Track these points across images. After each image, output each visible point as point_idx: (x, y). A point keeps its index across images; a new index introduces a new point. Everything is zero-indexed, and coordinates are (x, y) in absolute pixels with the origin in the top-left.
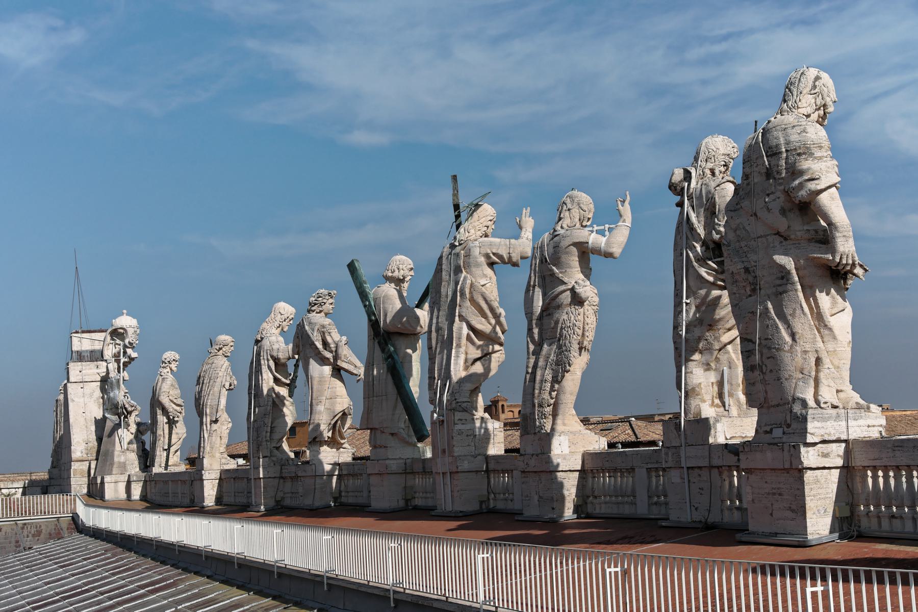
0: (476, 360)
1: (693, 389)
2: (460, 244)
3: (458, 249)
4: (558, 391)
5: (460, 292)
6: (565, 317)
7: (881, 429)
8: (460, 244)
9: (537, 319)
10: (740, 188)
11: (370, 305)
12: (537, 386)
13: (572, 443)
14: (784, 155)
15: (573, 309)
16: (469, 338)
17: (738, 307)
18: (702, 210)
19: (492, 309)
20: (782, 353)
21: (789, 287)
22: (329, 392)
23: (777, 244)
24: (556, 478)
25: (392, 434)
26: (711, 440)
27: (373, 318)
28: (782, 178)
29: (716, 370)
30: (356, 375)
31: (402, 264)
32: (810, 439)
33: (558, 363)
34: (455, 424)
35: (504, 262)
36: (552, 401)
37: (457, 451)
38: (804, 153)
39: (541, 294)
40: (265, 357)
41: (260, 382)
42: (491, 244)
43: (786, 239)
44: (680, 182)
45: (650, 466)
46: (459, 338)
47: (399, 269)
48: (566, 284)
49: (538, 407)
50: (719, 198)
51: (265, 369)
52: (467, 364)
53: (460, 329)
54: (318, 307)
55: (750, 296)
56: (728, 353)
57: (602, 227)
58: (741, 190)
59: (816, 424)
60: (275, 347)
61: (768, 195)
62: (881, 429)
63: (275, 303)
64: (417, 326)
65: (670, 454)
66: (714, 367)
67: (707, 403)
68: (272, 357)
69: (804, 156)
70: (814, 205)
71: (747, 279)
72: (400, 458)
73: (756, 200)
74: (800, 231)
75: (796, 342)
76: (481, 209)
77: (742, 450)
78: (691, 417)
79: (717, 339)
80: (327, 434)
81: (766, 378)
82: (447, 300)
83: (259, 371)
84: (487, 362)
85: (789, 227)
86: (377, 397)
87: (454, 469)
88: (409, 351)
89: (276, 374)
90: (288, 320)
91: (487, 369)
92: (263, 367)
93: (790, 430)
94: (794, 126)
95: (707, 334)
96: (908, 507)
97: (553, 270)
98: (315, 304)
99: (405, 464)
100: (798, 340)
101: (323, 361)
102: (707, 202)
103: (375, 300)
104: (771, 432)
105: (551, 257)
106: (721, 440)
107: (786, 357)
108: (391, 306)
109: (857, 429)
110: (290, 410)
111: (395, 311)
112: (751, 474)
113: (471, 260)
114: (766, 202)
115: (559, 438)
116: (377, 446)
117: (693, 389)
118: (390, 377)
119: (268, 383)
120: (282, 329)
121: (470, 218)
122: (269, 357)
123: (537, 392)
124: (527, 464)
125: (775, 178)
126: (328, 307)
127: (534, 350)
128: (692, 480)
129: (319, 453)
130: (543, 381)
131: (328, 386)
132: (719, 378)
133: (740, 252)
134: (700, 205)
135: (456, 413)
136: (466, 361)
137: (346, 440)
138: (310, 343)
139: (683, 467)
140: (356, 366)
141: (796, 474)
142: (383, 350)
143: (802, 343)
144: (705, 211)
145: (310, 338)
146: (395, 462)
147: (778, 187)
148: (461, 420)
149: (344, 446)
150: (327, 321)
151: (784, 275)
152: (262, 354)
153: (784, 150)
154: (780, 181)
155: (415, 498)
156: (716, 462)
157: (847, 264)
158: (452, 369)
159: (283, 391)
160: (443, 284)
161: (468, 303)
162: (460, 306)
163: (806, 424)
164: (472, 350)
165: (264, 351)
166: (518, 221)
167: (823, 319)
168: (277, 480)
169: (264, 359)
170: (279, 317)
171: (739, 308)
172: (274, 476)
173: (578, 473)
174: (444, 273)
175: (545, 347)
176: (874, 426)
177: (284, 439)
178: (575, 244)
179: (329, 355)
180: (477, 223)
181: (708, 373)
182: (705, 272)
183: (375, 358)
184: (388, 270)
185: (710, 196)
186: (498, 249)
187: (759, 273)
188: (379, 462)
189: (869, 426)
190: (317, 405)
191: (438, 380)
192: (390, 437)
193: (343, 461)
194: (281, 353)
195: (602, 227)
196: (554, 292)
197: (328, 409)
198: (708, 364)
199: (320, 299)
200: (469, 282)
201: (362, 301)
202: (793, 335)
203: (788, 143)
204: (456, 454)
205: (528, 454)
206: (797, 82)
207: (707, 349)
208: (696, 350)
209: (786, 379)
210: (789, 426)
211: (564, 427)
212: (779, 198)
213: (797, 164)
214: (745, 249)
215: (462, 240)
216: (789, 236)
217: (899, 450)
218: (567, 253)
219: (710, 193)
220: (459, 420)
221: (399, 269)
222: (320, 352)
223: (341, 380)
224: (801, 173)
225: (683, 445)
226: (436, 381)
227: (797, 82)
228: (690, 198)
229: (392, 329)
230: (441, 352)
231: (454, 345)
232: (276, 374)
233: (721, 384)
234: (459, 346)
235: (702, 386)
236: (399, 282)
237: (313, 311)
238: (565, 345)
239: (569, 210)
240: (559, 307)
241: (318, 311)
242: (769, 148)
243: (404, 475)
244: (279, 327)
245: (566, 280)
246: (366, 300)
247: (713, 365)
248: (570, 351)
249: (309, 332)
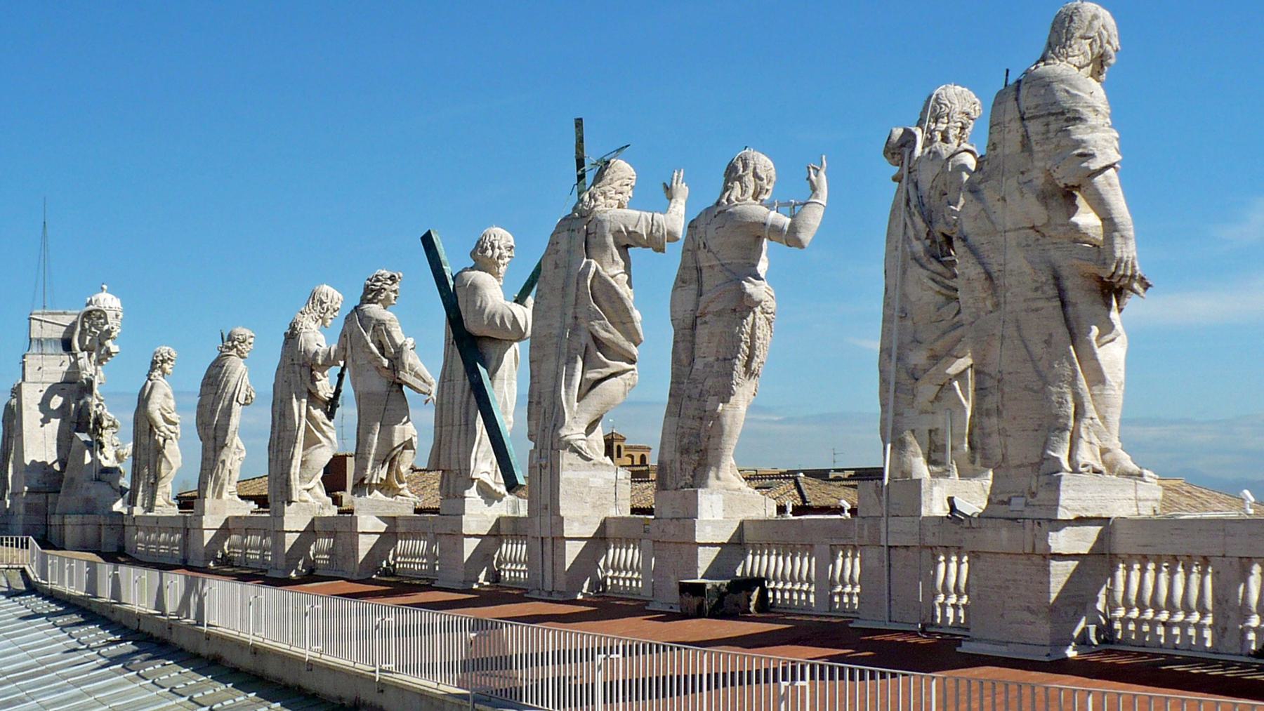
7: (1155, 504)
10: (984, 161)
13: (728, 506)
26: (925, 512)
30: (424, 393)
32: (1062, 514)
58: (986, 163)
59: (1072, 494)
62: (1155, 504)
65: (866, 527)
93: (1034, 501)
104: (1008, 503)
124: (663, 531)
137: (406, 485)
139: (883, 546)
141: (1036, 559)
149: (401, 492)
156: (930, 540)
157: (1124, 276)
176: (1147, 500)
186: (636, 227)
199: (379, 284)
200: (592, 270)
210: (1033, 495)
225: (885, 515)
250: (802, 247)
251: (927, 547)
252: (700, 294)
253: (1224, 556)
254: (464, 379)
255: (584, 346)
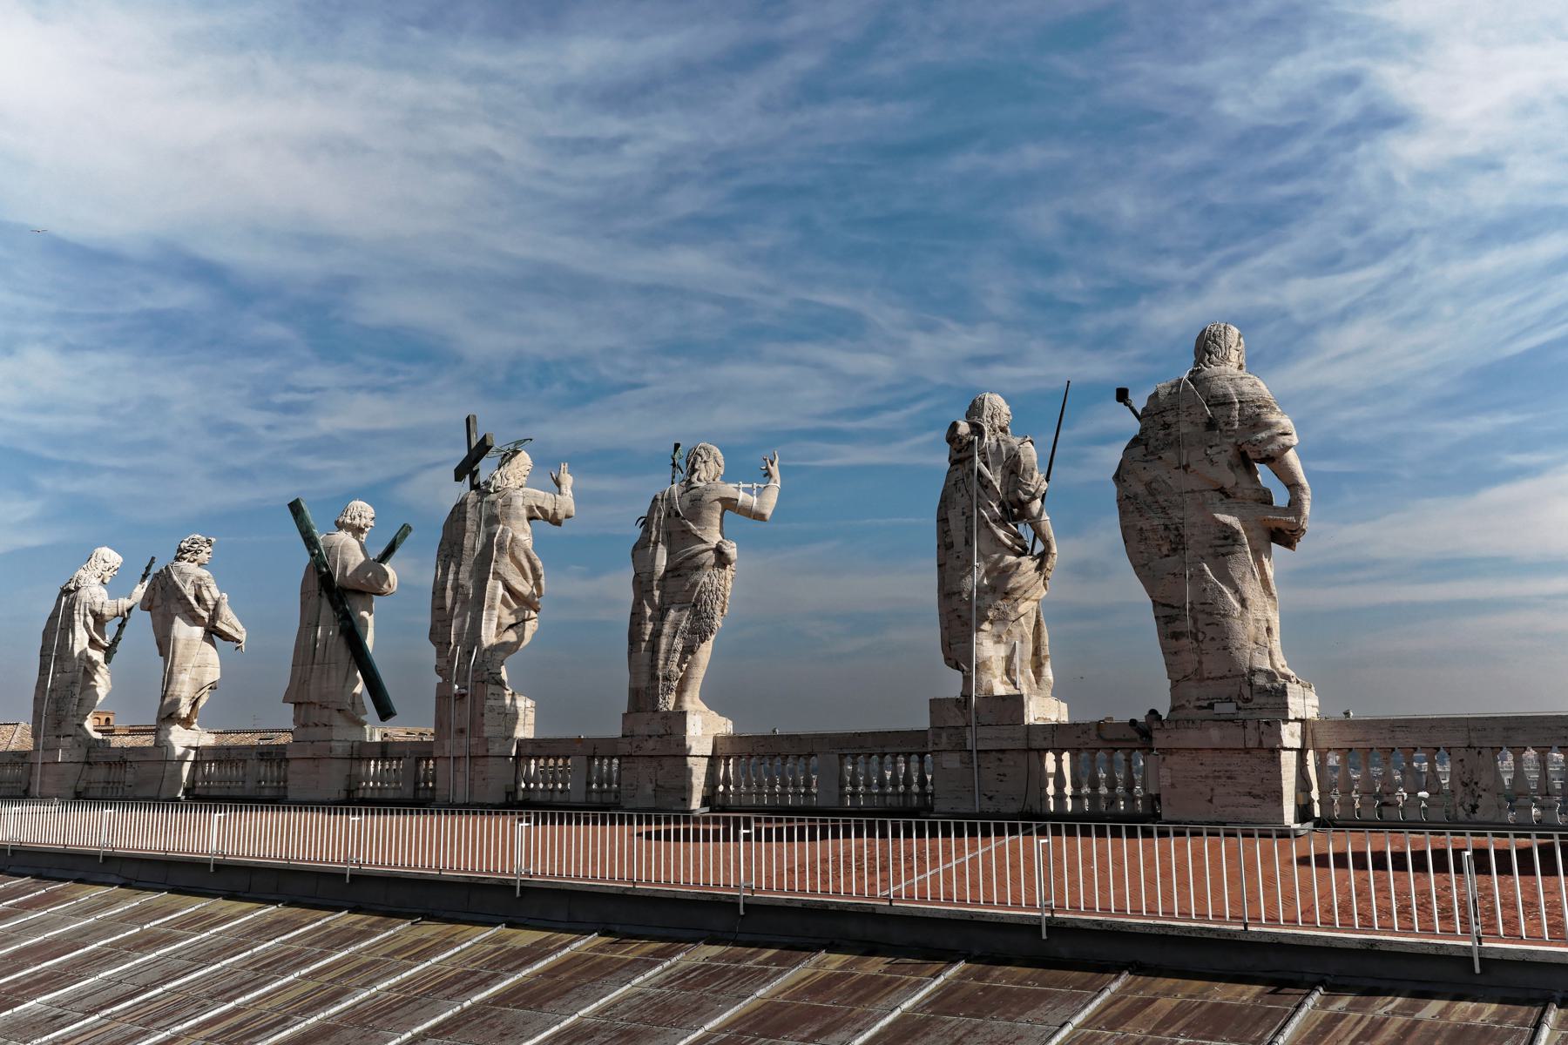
0: (511, 626)
1: (984, 662)
2: (496, 492)
3: (493, 497)
4: (689, 663)
5: (497, 545)
6: (706, 579)
8: (496, 492)
9: (659, 580)
11: (320, 554)
12: (662, 656)
14: (1238, 406)
15: (716, 572)
16: (504, 602)
17: (1147, 568)
18: (1000, 467)
19: (534, 569)
20: (1230, 620)
21: (1237, 548)
22: (198, 659)
23: (1216, 500)
24: (686, 764)
25: (339, 710)
27: (324, 570)
28: (1234, 430)
29: (1005, 643)
31: (363, 511)
33: (692, 631)
34: (488, 699)
35: (546, 519)
36: (681, 674)
37: (488, 731)
38: (1265, 407)
39: (665, 551)
40: (82, 612)
41: (70, 642)
42: (535, 496)
43: (1228, 496)
44: (967, 435)
45: (846, 752)
46: (493, 599)
47: (360, 516)
48: (705, 542)
49: (663, 680)
50: (1025, 456)
51: (79, 626)
52: (501, 630)
53: (496, 588)
54: (192, 555)
55: (1167, 556)
56: (1021, 625)
57: (750, 486)
60: (99, 600)
61: (1211, 447)
63: (97, 547)
64: (384, 582)
66: (1005, 640)
67: (998, 679)
68: (92, 612)
69: (1265, 410)
70: (1279, 462)
71: (1168, 537)
72: (346, 740)
73: (1188, 453)
75: (1246, 608)
76: (519, 455)
77: (1159, 727)
78: (982, 694)
79: (1015, 609)
80: (185, 711)
81: (1203, 646)
82: (474, 554)
83: (69, 625)
84: (521, 630)
85: (1236, 484)
86: (318, 664)
87: (481, 752)
88: (365, 614)
89: (94, 633)
90: (113, 569)
91: (521, 638)
92: (77, 623)
93: (1250, 705)
95: (1000, 602)
96: (1124, 799)
97: (689, 526)
98: (189, 551)
99: (352, 748)
100: (1249, 608)
101: (194, 619)
102: (1007, 459)
103: (329, 549)
104: (1211, 706)
105: (686, 511)
106: (1032, 721)
107: (1237, 625)
108: (353, 558)
110: (105, 680)
111: (358, 563)
112: (1171, 755)
113: (511, 511)
114: (1207, 455)
115: (693, 717)
116: (310, 724)
117: (984, 662)
118: (342, 640)
119: (81, 644)
120: (102, 581)
121: (507, 464)
122: (88, 612)
123: (661, 663)
125: (1221, 430)
126: (203, 557)
127: (652, 614)
128: (983, 765)
129: (170, 733)
130: (670, 651)
131: (197, 651)
132: (1009, 652)
133: (1153, 507)
134: (997, 463)
135: (490, 686)
136: (499, 625)
138: (179, 596)
140: (237, 630)
141: (1265, 754)
142: (335, 608)
143: (1253, 611)
144: (1003, 468)
145: (181, 590)
146: (340, 744)
147: (1226, 440)
150: (204, 573)
151: (1230, 536)
152: (77, 607)
153: (1236, 400)
154: (1230, 433)
155: (358, 789)
158: (483, 634)
159: (98, 656)
160: (467, 534)
161: (507, 559)
162: (496, 561)
163: (1286, 699)
164: (506, 612)
165: (80, 605)
166: (554, 475)
167: (1269, 587)
168: (80, 766)
169: (79, 613)
170: (101, 565)
171: (1150, 569)
172: (76, 761)
173: (707, 759)
174: (468, 523)
175: (672, 614)
177: (88, 717)
178: (723, 500)
179: (205, 614)
180: (516, 471)
181: (998, 645)
182: (1005, 535)
183: (321, 618)
184: (346, 516)
185: (1013, 453)
187: (1187, 532)
188: (316, 743)
190: (180, 673)
191: (456, 646)
192: (336, 713)
193: (204, 744)
194: (107, 609)
195: (750, 486)
196: (690, 550)
197: (193, 679)
198: (999, 636)
199: (196, 546)
201: (309, 549)
202: (1243, 602)
203: (1241, 394)
204: (486, 735)
205: (638, 735)
206: (1222, 334)
207: (1000, 620)
208: (987, 620)
209: (1237, 649)
211: (694, 706)
212: (1225, 451)
213: (1263, 416)
214: (1165, 504)
215: (499, 487)
216: (1234, 494)
217: (1400, 731)
218: (710, 508)
219: (1013, 450)
220: (493, 694)
221: (360, 516)
222: (193, 608)
223: (214, 645)
224: (1269, 426)
226: (452, 647)
227: (1222, 334)
228: (983, 454)
229: (351, 585)
230: (462, 615)
231: (486, 606)
232: (94, 633)
233: (1009, 660)
234: (491, 607)
235: (993, 660)
236: (357, 531)
237: (184, 559)
238: (705, 611)
239: (705, 462)
240: (698, 568)
241: (192, 559)
242: (1212, 397)
243: (349, 761)
244: (99, 577)
245: (705, 538)
246: (315, 548)
247: (1004, 637)
248: (713, 618)
249: (180, 584)
250: (765, 520)
251: (1035, 750)
253: (1469, 747)
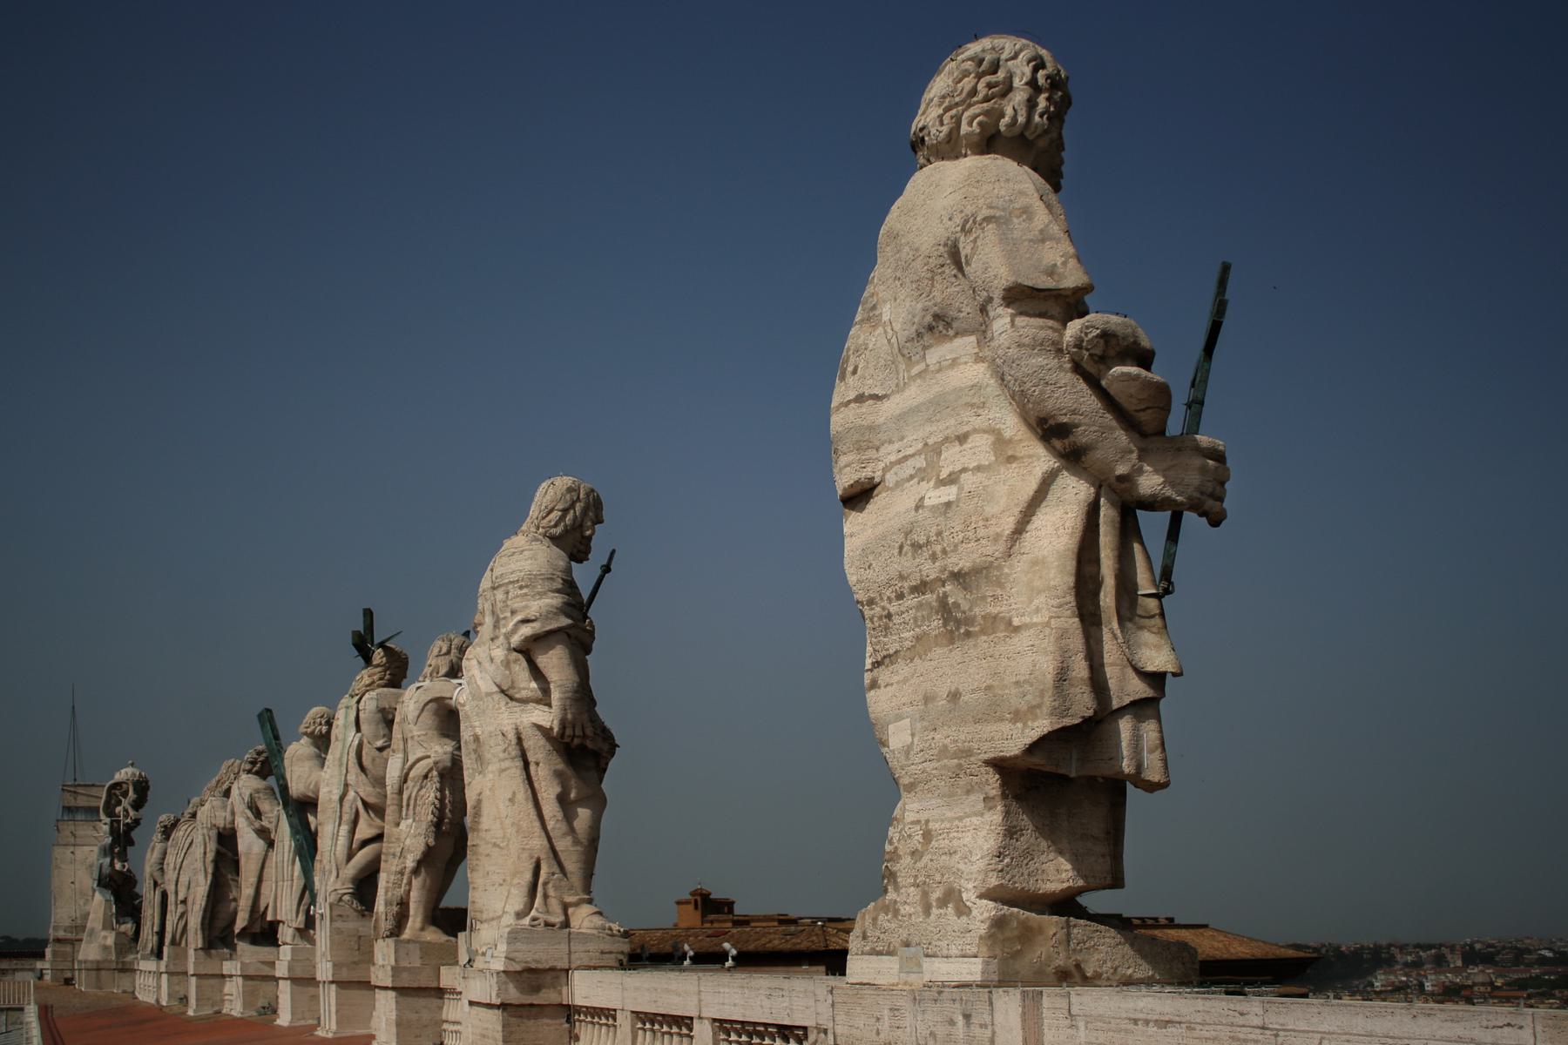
23: (503, 703)
74: (524, 689)
94: (522, 551)
109: (582, 955)
148: (340, 916)
189: (602, 953)
252: (406, 760)
254: (290, 841)
255: (354, 810)
